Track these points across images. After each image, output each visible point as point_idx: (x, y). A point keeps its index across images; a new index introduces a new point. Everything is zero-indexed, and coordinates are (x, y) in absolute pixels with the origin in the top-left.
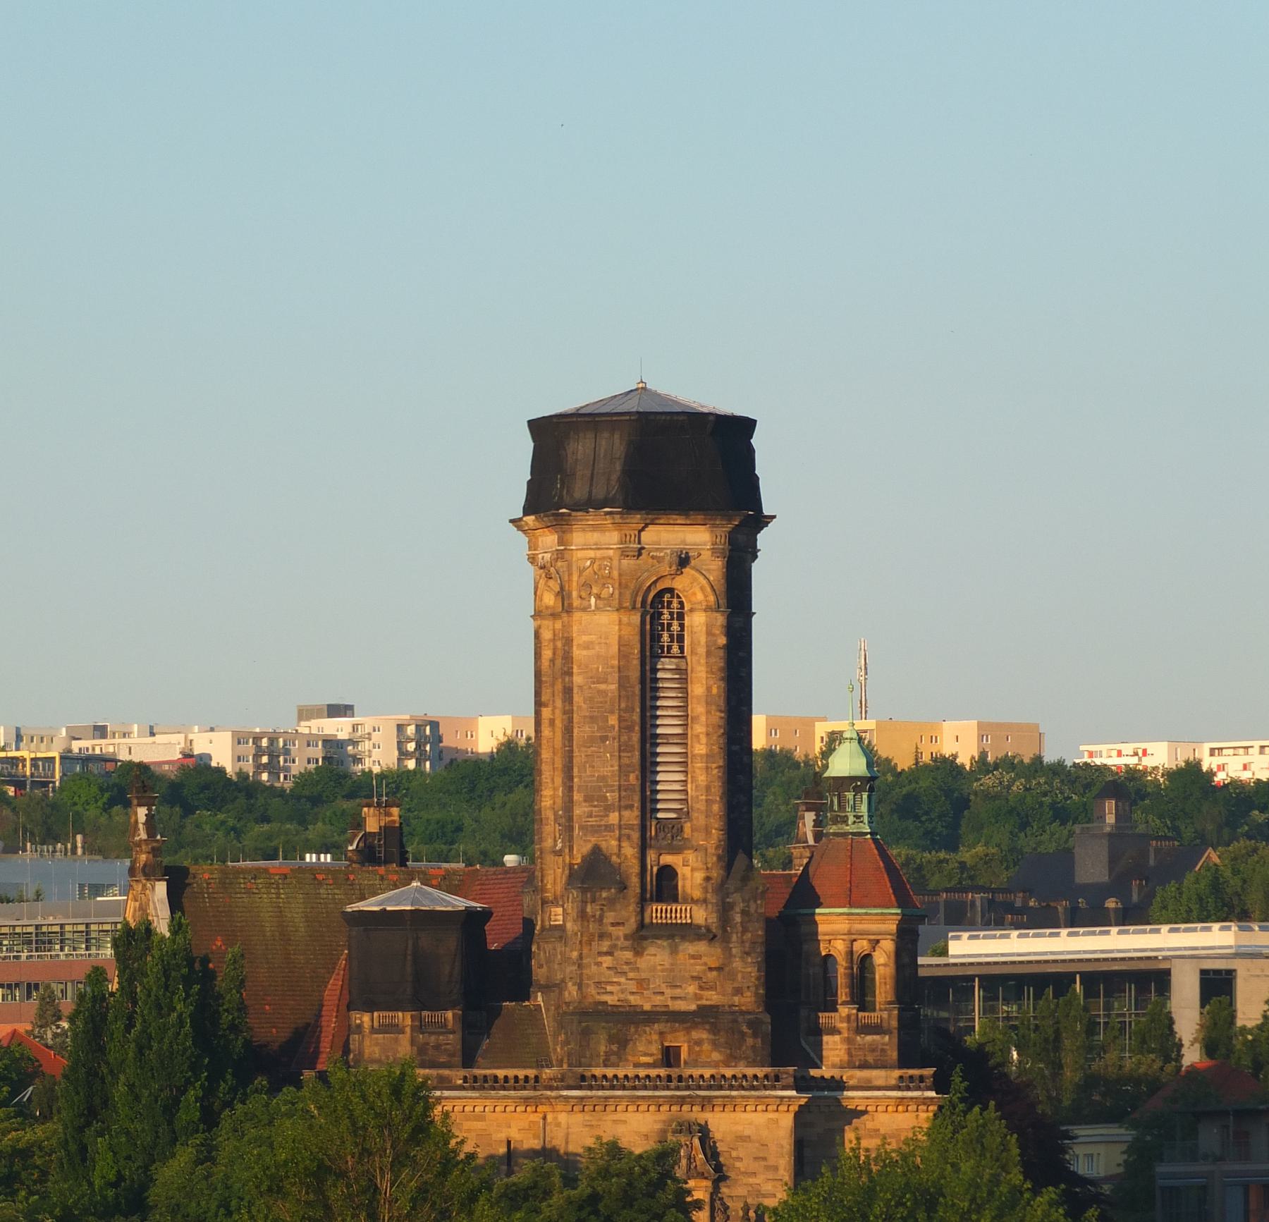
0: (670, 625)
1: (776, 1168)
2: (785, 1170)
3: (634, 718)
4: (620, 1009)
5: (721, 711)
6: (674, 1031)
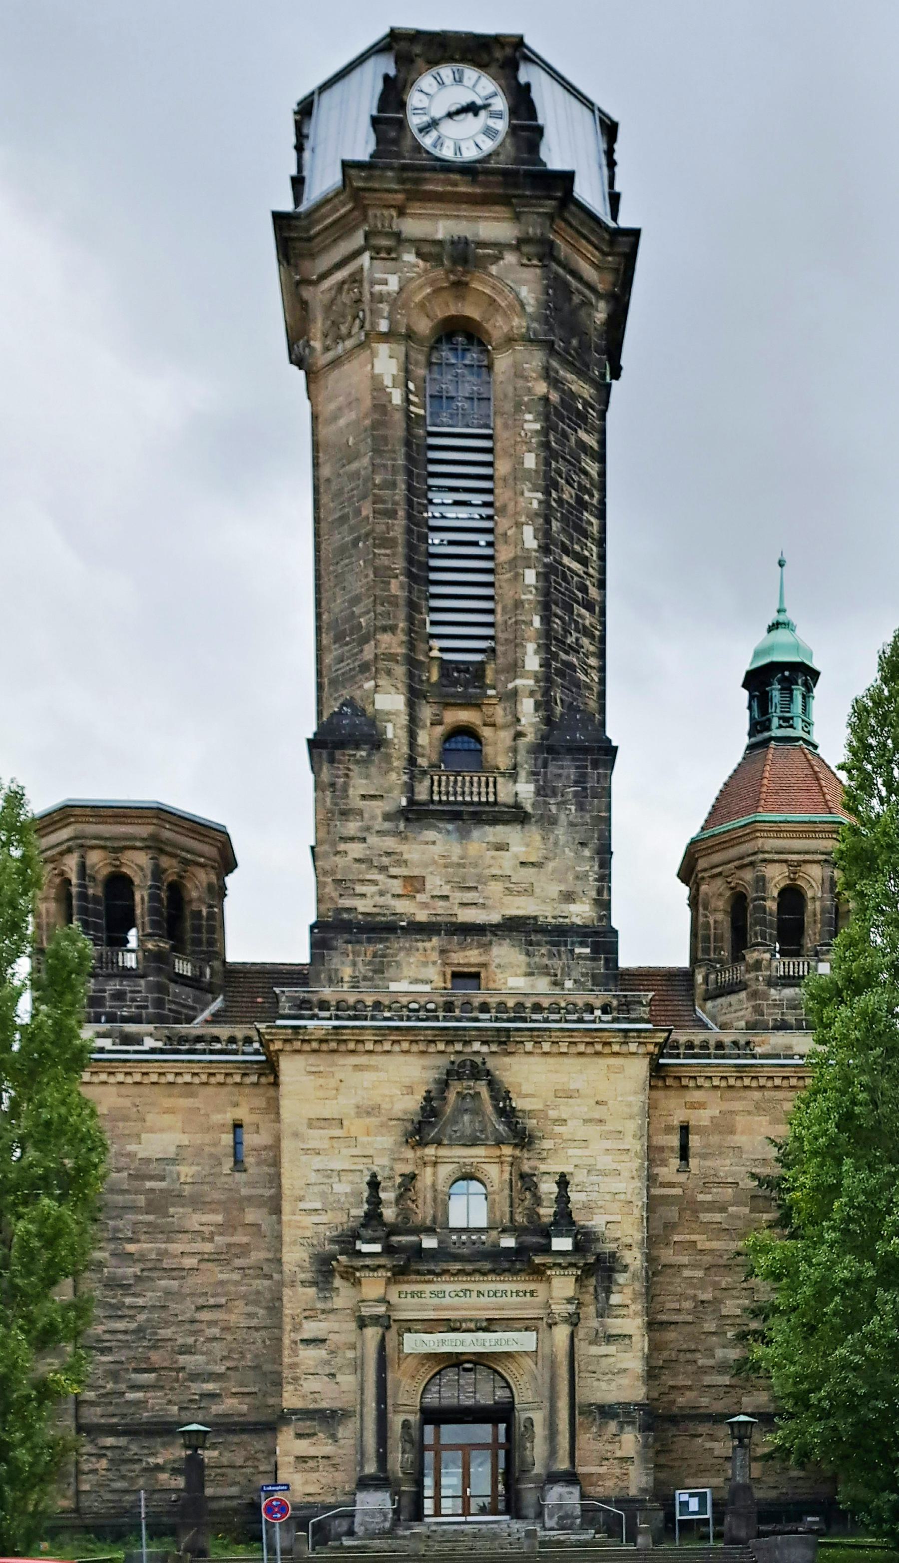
3: (397, 498)
4: (378, 919)
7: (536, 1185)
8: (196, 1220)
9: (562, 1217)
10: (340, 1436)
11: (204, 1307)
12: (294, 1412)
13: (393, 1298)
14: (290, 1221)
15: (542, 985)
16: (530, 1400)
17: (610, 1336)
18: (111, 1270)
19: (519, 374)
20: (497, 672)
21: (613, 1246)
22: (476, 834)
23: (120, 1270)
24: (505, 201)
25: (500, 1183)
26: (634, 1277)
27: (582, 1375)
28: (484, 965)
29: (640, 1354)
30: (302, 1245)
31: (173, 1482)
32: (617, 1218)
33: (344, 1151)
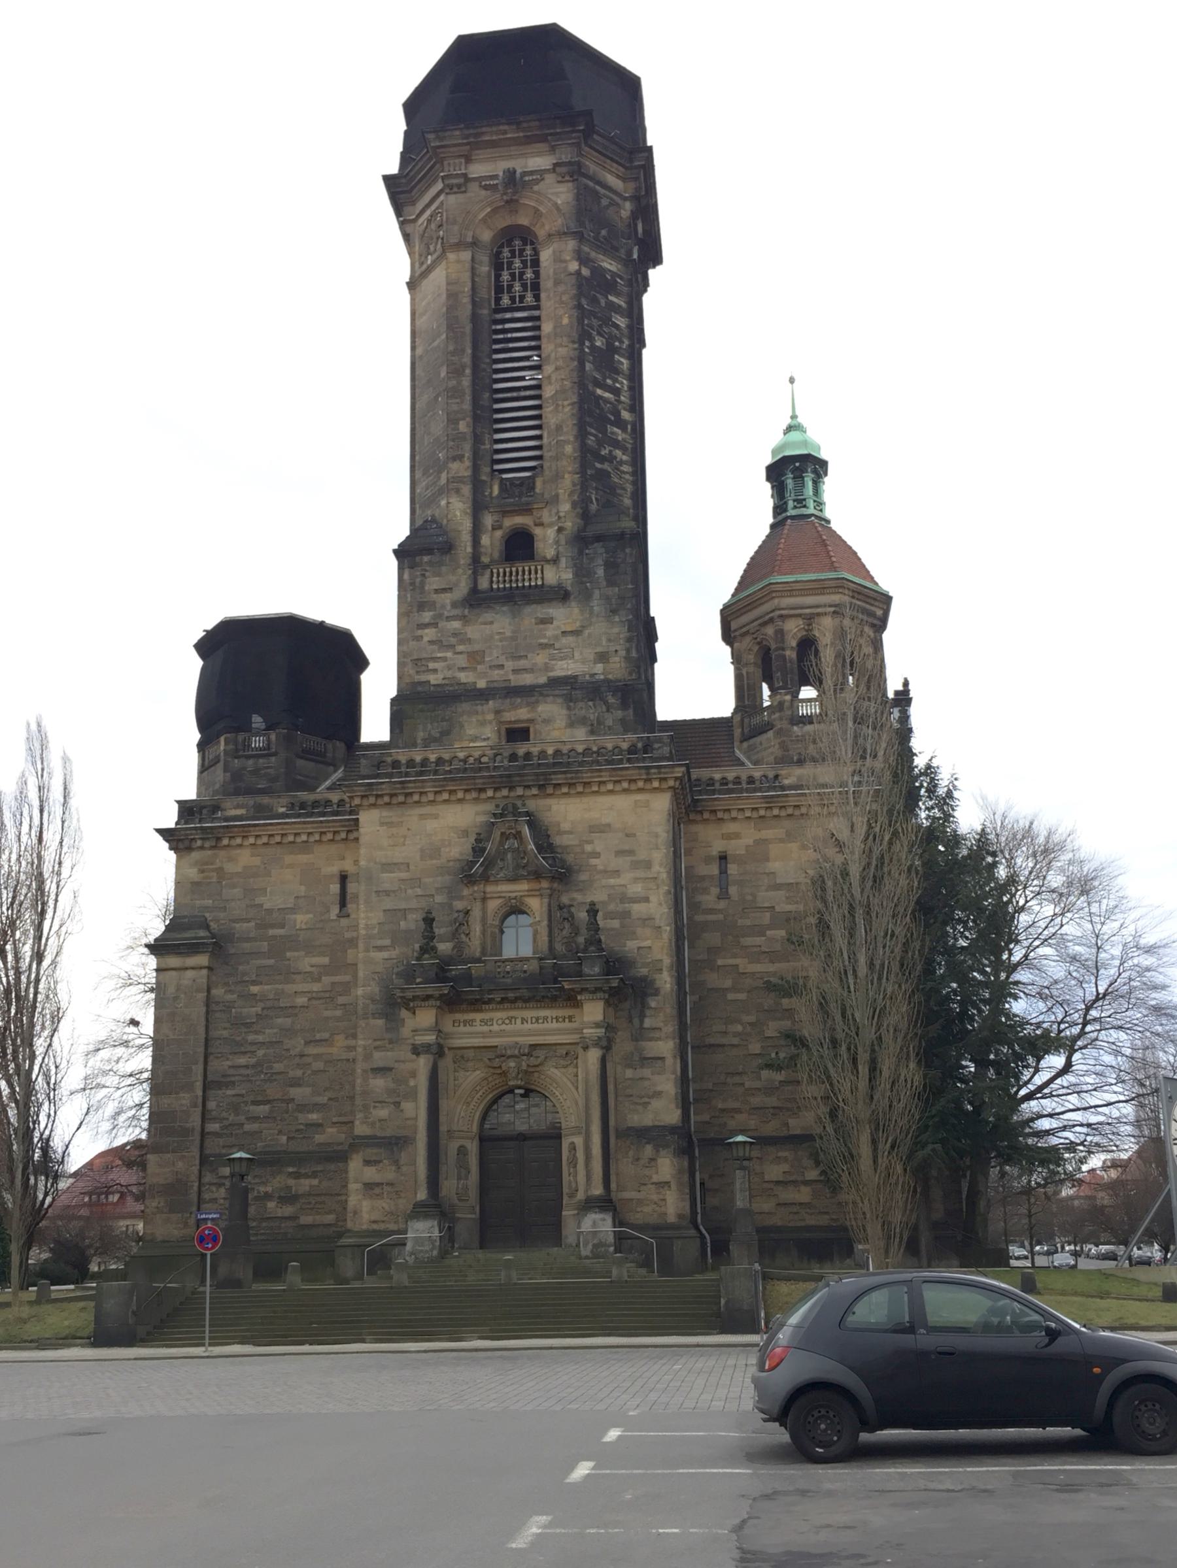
0: (522, 274)
1: (648, 865)
2: (661, 865)
5: (573, 342)
6: (515, 707)
8: (307, 963)
11: (311, 1041)
15: (581, 733)
18: (239, 1010)
19: (558, 259)
20: (544, 482)
22: (528, 609)
23: (245, 1010)
24: (543, 139)
28: (531, 721)
31: (279, 1210)
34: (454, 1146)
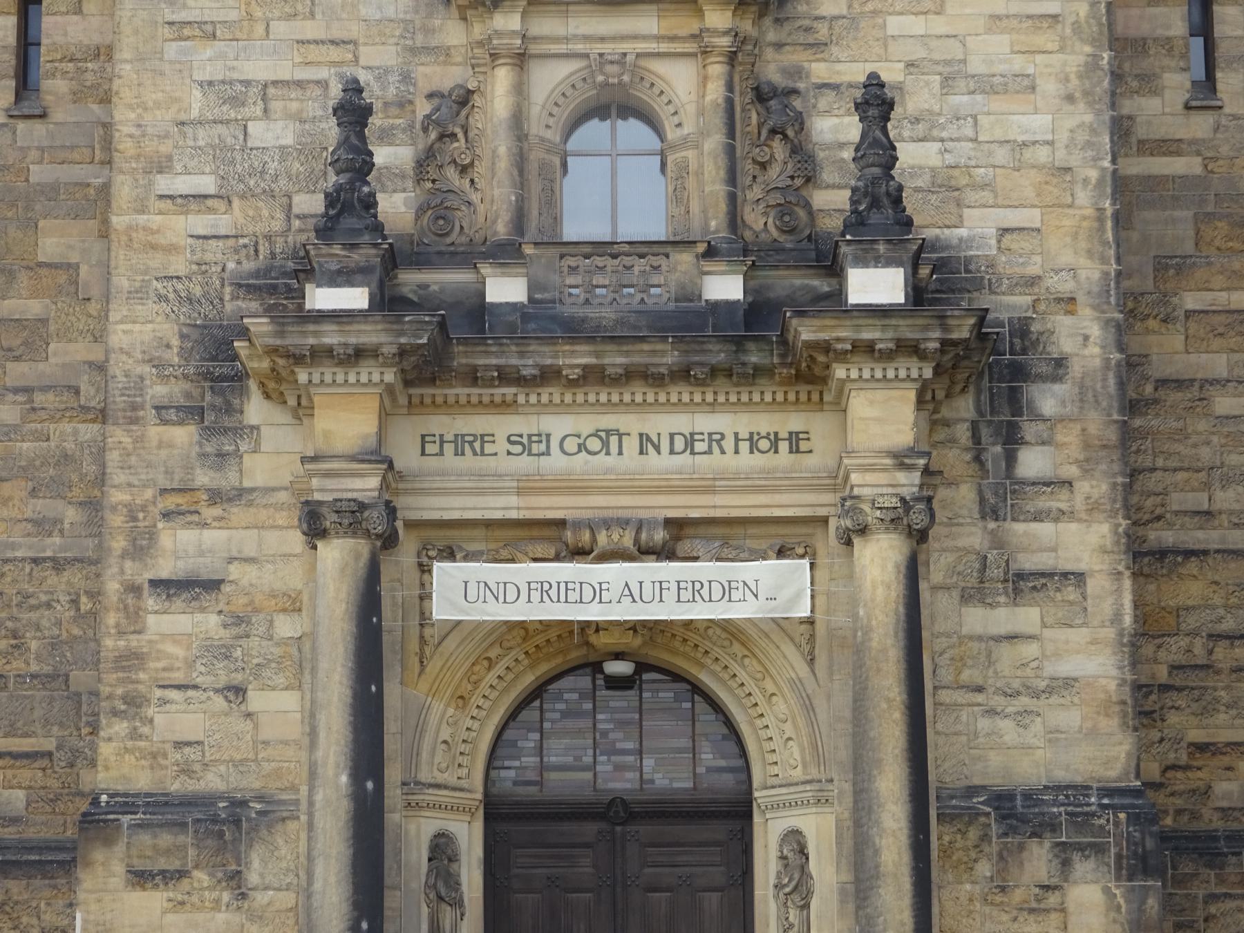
7: (800, 121)
9: (875, 203)
10: (253, 878)
12: (127, 803)
13: (406, 456)
14: (130, 228)
16: (798, 774)
17: (1021, 576)
21: (1020, 301)
25: (701, 112)
26: (1083, 394)
27: (945, 696)
29: (1110, 633)
30: (161, 298)
32: (1029, 217)
33: (280, 29)
34: (421, 830)
